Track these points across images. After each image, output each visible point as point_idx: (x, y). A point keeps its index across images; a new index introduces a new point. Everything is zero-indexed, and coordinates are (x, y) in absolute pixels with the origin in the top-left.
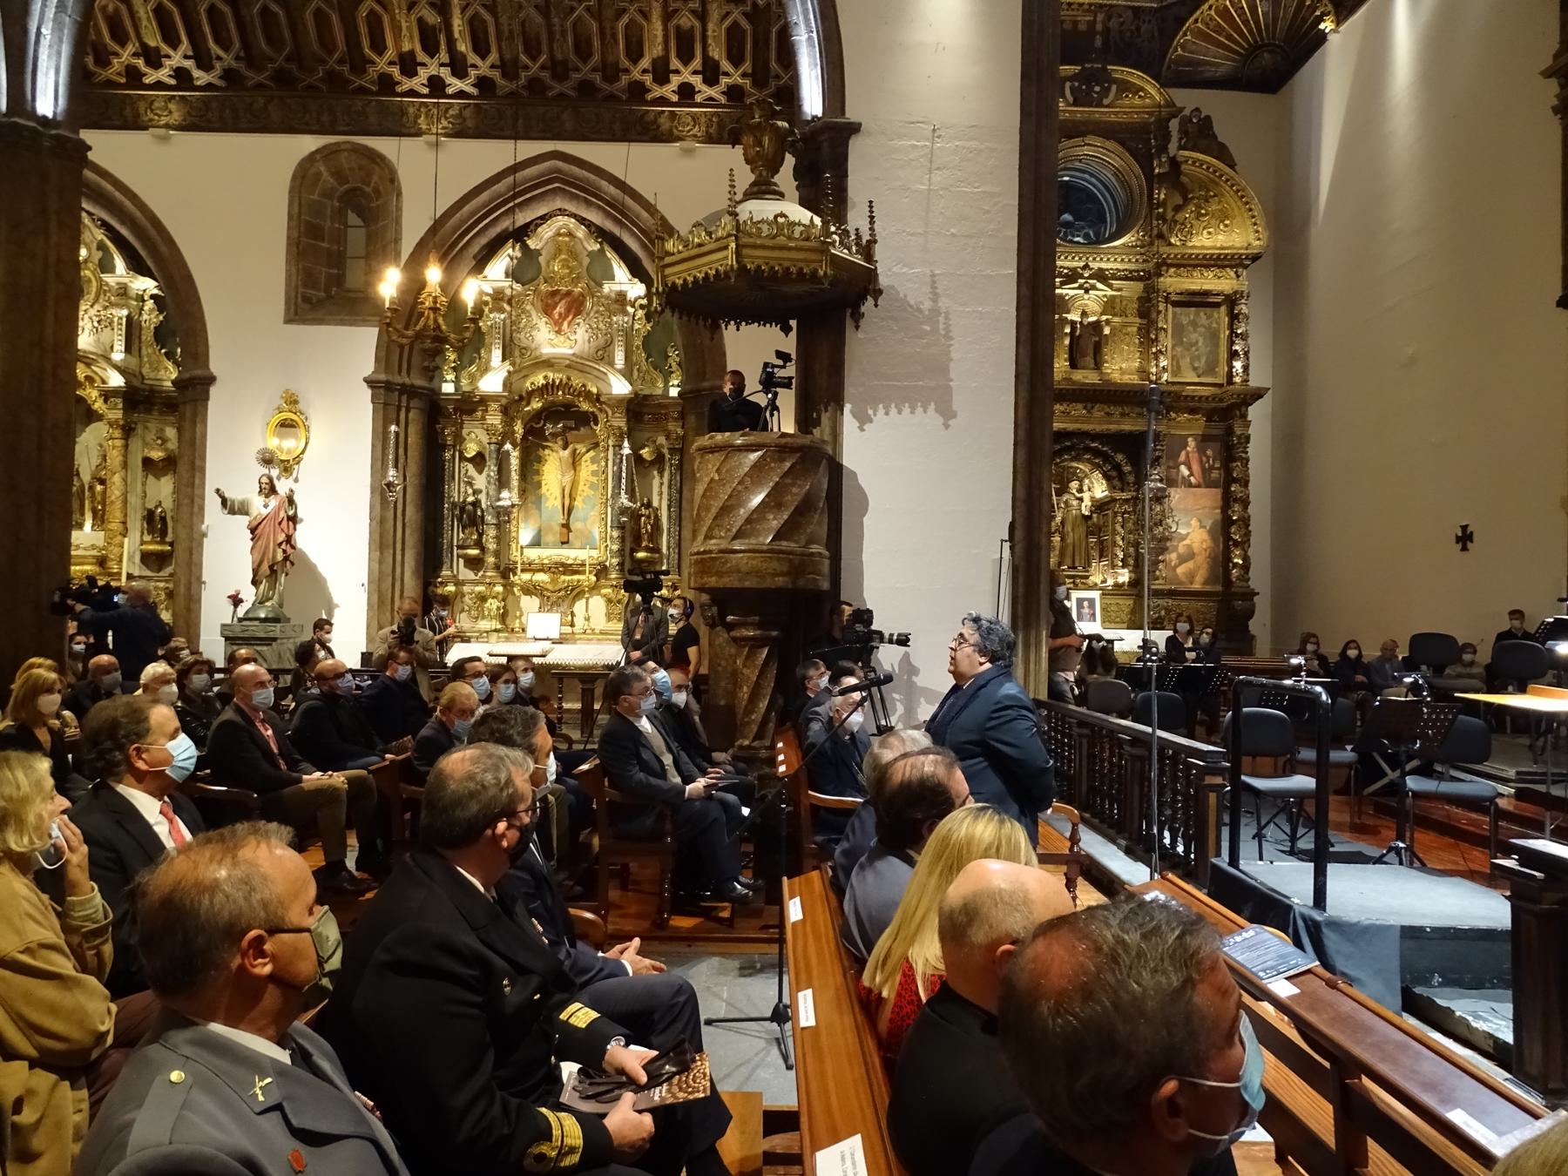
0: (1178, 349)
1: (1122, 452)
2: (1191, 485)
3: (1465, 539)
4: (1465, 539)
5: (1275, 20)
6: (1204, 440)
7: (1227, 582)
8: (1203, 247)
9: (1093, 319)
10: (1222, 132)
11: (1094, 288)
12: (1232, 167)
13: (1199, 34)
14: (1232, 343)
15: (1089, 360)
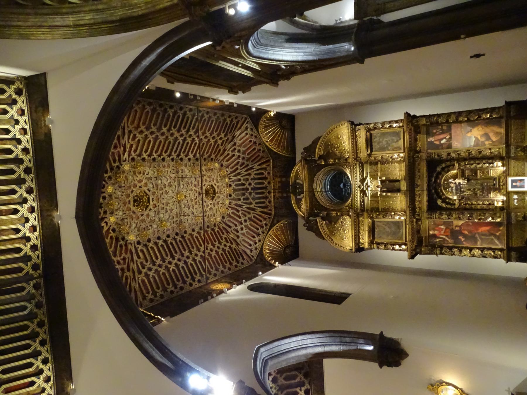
0: (390, 148)
1: (436, 168)
2: (450, 138)
3: (478, 56)
4: (478, 56)
5: (272, 125)
6: (428, 134)
7: (501, 117)
8: (349, 144)
9: (379, 183)
10: (308, 143)
11: (367, 184)
12: (319, 138)
13: (278, 147)
14: (386, 128)
15: (396, 184)
